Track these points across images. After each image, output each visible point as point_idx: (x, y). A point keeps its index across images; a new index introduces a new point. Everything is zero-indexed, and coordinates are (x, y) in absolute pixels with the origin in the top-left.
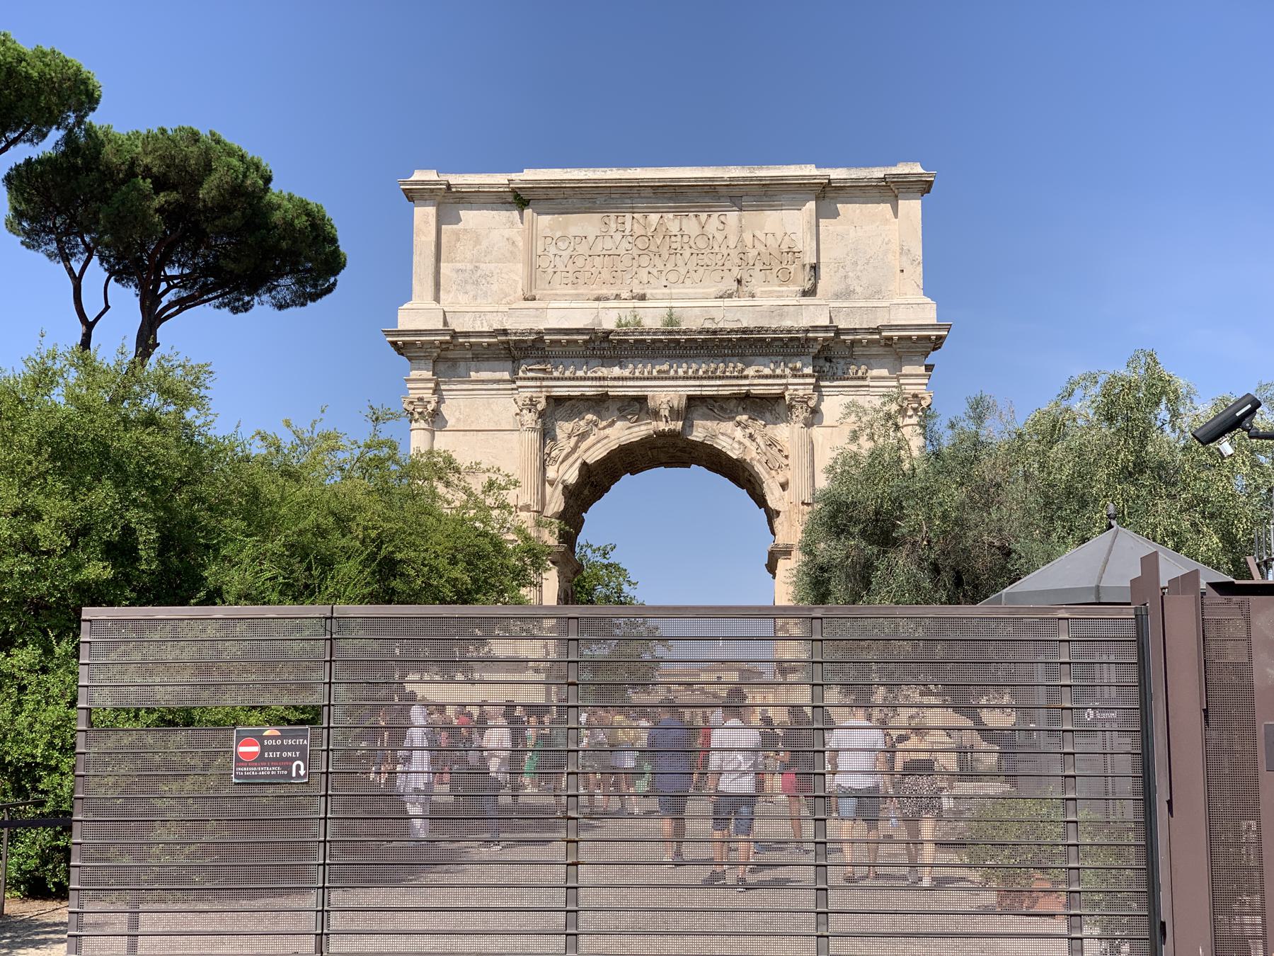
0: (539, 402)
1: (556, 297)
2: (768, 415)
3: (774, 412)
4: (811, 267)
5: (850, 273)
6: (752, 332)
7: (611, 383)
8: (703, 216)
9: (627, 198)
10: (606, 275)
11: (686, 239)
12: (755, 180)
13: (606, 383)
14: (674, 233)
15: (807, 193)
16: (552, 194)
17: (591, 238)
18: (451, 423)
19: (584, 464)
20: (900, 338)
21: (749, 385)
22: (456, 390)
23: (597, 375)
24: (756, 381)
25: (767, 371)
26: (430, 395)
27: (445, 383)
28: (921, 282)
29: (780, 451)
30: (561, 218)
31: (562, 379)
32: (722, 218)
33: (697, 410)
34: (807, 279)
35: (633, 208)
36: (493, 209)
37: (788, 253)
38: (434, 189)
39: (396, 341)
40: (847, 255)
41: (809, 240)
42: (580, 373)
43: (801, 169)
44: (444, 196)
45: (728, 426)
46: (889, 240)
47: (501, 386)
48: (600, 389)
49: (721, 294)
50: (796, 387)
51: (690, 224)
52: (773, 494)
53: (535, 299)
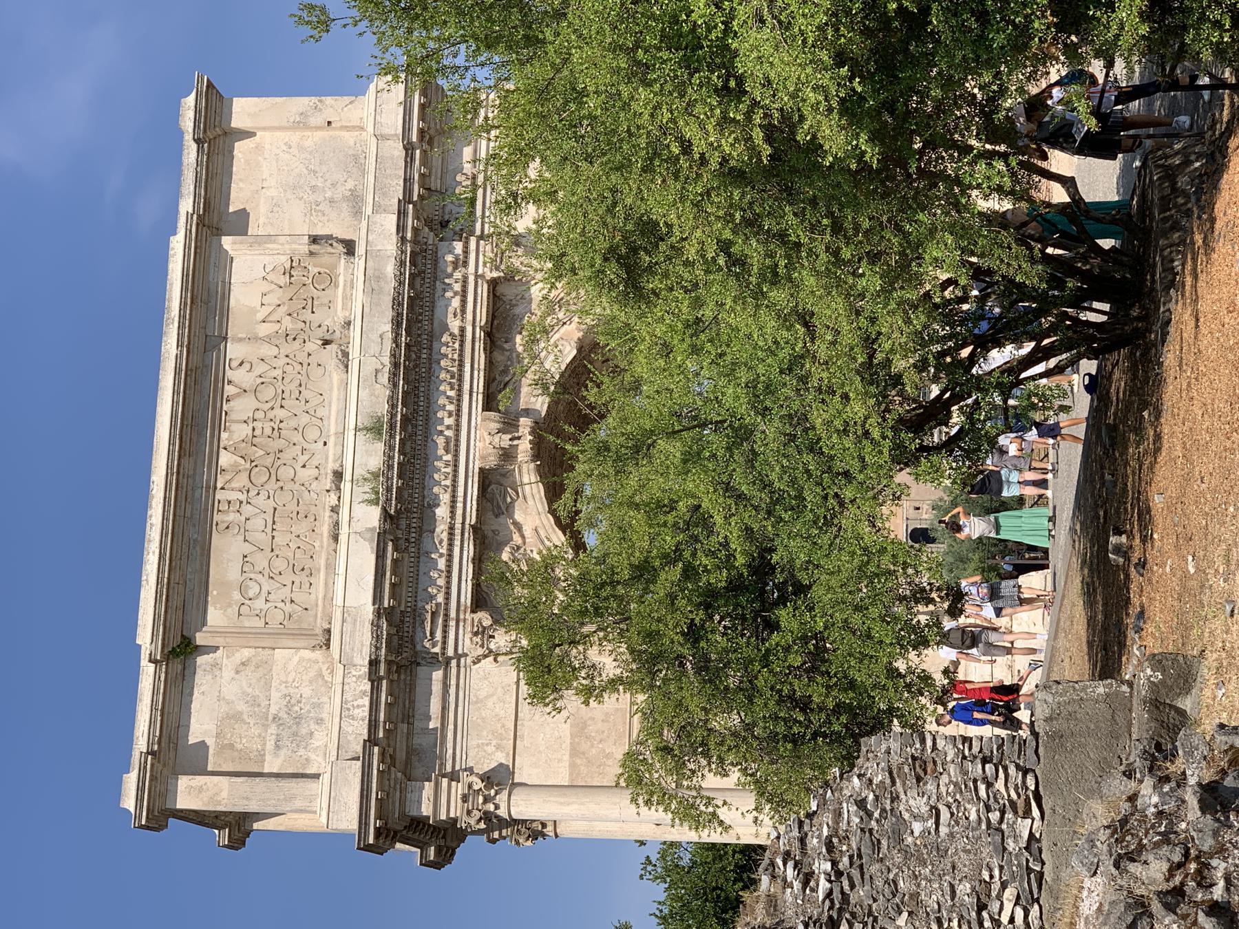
0: (480, 622)
1: (329, 598)
2: (517, 311)
3: (514, 302)
6: (399, 315)
7: (459, 519)
8: (229, 390)
10: (302, 528)
11: (259, 415)
12: (185, 312)
13: (458, 526)
15: (210, 247)
16: (177, 601)
17: (247, 548)
18: (502, 758)
20: (422, 117)
22: (454, 749)
23: (446, 540)
24: (469, 316)
25: (456, 303)
26: (460, 784)
27: (443, 765)
28: (347, 99)
30: (213, 592)
32: (234, 364)
34: (330, 249)
35: (208, 487)
36: (191, 694)
37: (291, 276)
38: (151, 775)
41: (275, 246)
43: (175, 255)
44: (164, 765)
46: (286, 144)
47: (453, 682)
48: (466, 535)
49: (342, 367)
50: (481, 263)
53: (329, 631)
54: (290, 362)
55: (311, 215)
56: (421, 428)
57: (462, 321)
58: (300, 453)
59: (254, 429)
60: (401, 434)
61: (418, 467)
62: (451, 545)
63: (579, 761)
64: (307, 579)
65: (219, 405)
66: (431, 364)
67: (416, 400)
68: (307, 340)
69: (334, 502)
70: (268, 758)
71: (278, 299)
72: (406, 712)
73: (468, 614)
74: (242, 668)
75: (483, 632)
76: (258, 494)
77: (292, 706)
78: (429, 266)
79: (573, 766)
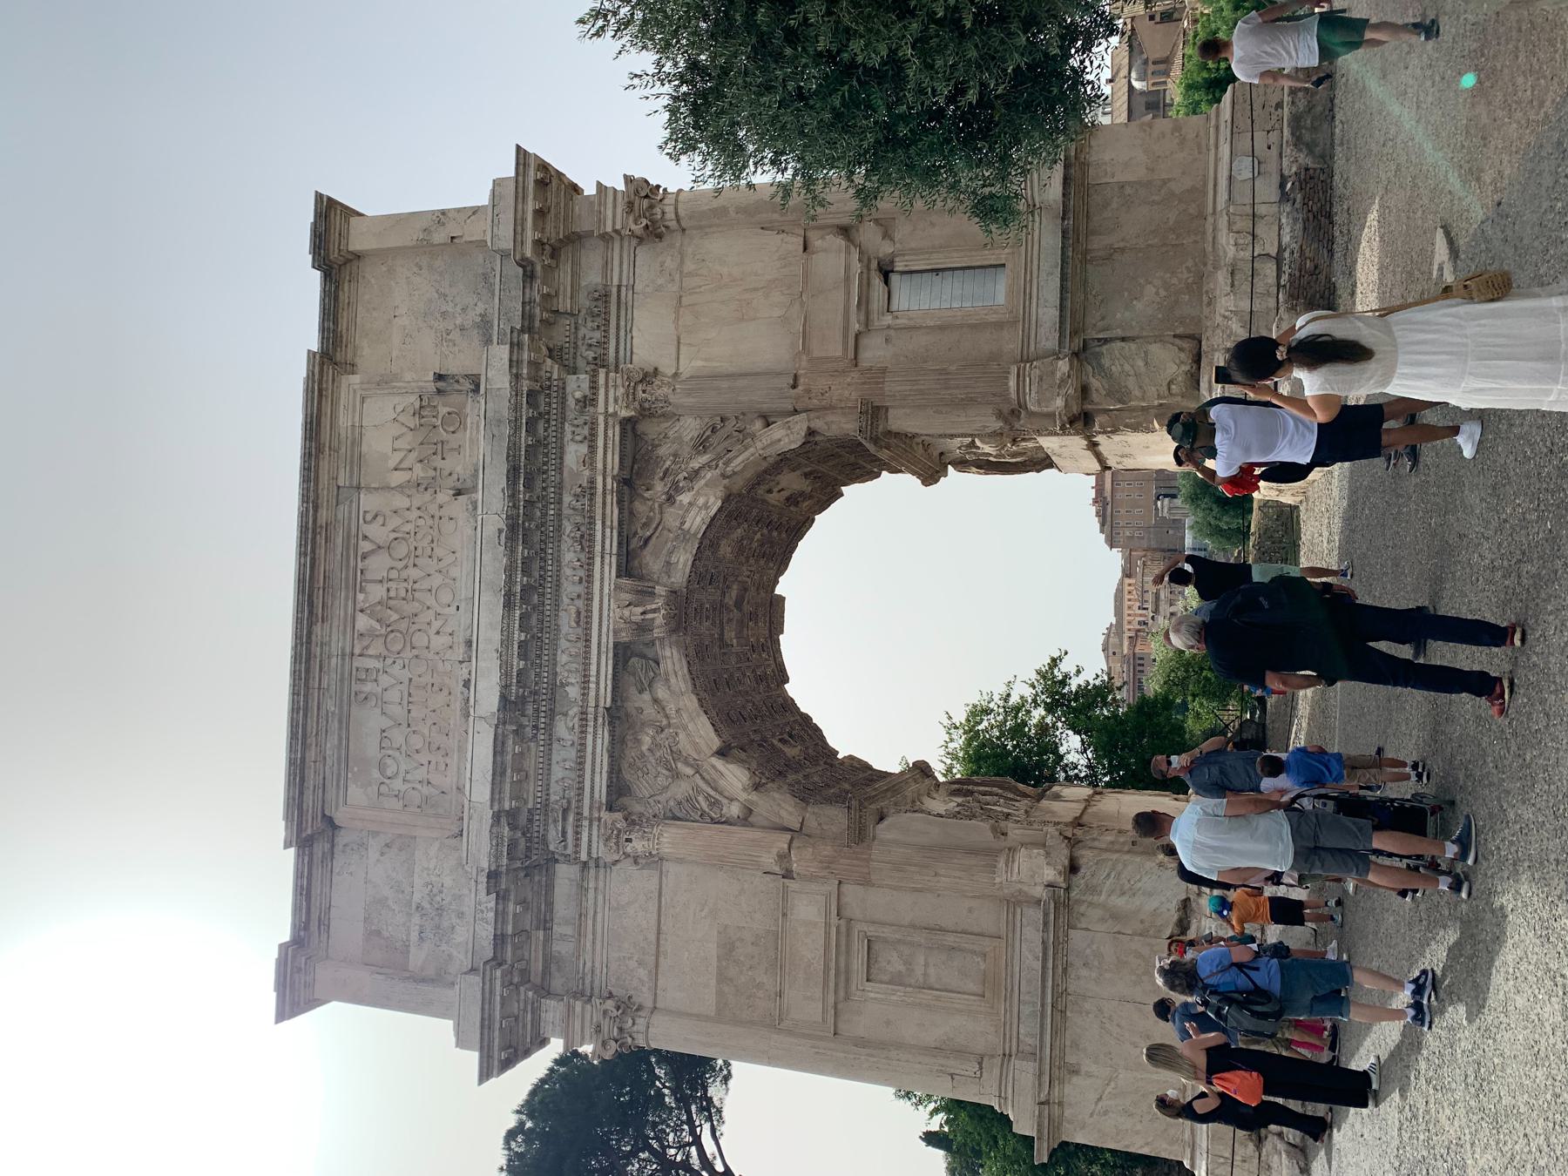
5: (457, 322)
7: (592, 703)
8: (365, 546)
9: (329, 663)
11: (394, 574)
12: (310, 464)
13: (591, 710)
17: (389, 723)
19: (722, 753)
23: (576, 726)
24: (600, 466)
29: (714, 430)
32: (369, 517)
33: (647, 564)
34: (457, 387)
39: (500, 1061)
40: (431, 328)
45: (671, 517)
48: (600, 720)
50: (611, 400)
51: (378, 565)
52: (780, 440)
54: (422, 515)
55: (442, 345)
56: (549, 596)
59: (388, 590)
60: (521, 607)
61: (547, 641)
63: (726, 989)
65: (352, 563)
67: (542, 564)
69: (466, 677)
70: (412, 949)
71: (409, 444)
72: (542, 917)
73: (602, 814)
74: (387, 850)
75: (618, 836)
76: (394, 662)
77: (435, 895)
79: (720, 994)
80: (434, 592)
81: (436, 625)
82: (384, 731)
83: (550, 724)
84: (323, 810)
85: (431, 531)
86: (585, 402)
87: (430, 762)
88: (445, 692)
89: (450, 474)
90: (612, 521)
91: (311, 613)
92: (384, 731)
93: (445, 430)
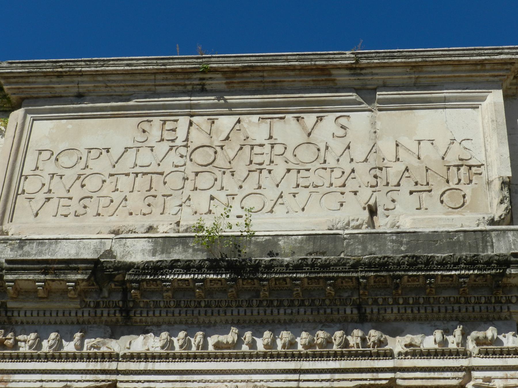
4: (503, 183)
7: (123, 366)
8: (310, 119)
11: (278, 149)
12: (398, 57)
13: (113, 366)
14: (258, 142)
21: (393, 370)
31: (32, 358)
42: (69, 347)
49: (339, 226)
57: (400, 354)
58: (229, 193)
59: (261, 145)
62: (89, 357)
64: (72, 210)
66: (339, 321)
67: (286, 303)
68: (374, 189)
69: (161, 229)
76: (182, 156)
78: (477, 307)
80: (258, 191)
81: (221, 196)
82: (108, 152)
83: (101, 322)
84: (27, 98)
85: (327, 184)
86: (485, 344)
87: (70, 198)
88: (146, 210)
89: (393, 201)
90: (339, 380)
91: (236, 71)
92: (108, 152)
93: (444, 193)
